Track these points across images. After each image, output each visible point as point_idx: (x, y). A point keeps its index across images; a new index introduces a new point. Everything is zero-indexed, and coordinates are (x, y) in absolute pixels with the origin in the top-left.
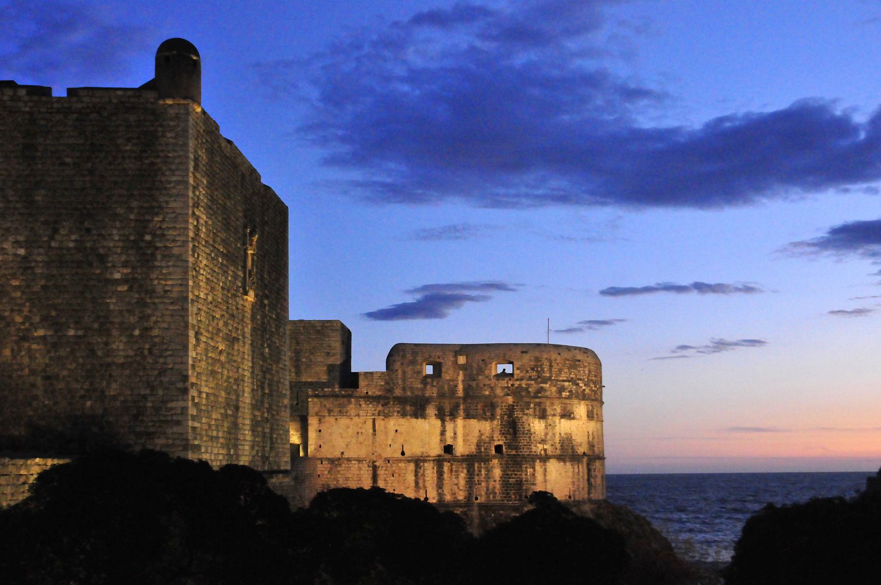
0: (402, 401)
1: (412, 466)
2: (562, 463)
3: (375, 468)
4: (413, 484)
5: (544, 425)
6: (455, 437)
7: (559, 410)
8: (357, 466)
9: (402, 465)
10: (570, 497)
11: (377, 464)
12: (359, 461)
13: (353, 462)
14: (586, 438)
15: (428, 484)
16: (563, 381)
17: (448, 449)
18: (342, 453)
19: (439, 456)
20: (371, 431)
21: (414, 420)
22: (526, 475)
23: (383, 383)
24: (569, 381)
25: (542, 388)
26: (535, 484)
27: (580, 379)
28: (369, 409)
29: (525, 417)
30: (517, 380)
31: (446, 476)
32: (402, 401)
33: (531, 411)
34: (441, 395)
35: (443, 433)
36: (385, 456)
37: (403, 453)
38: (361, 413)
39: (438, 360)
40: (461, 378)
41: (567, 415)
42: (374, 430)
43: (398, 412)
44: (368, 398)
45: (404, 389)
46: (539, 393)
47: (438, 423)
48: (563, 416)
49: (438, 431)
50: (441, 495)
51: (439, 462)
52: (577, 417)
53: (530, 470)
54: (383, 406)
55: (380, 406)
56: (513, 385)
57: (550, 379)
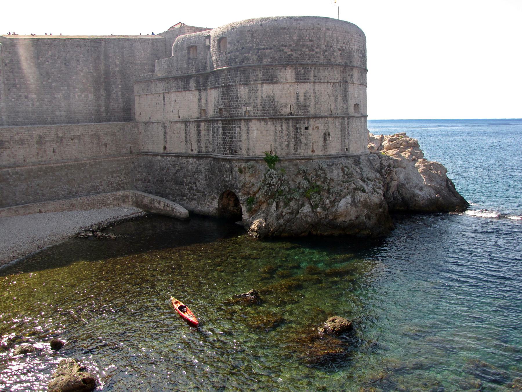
1: (183, 125)
2: (263, 123)
3: (165, 127)
4: (184, 139)
5: (247, 90)
6: (206, 104)
7: (260, 76)
9: (178, 125)
10: (271, 152)
11: (166, 125)
13: (155, 124)
14: (293, 100)
15: (192, 140)
16: (264, 49)
17: (202, 111)
18: (150, 118)
19: (198, 118)
20: (163, 101)
21: (184, 93)
22: (235, 133)
23: (166, 67)
24: (271, 49)
25: (245, 57)
26: (241, 141)
27: (285, 46)
28: (160, 87)
29: (234, 84)
30: (229, 53)
31: (203, 133)
32: (176, 78)
33: (238, 79)
35: (200, 100)
38: (157, 89)
39: (195, 45)
41: (271, 80)
42: (164, 102)
43: (175, 87)
45: (177, 70)
46: (243, 62)
47: (197, 93)
49: (196, 100)
50: (199, 147)
51: (198, 122)
52: (283, 80)
53: (237, 129)
56: (227, 58)
57: (250, 49)
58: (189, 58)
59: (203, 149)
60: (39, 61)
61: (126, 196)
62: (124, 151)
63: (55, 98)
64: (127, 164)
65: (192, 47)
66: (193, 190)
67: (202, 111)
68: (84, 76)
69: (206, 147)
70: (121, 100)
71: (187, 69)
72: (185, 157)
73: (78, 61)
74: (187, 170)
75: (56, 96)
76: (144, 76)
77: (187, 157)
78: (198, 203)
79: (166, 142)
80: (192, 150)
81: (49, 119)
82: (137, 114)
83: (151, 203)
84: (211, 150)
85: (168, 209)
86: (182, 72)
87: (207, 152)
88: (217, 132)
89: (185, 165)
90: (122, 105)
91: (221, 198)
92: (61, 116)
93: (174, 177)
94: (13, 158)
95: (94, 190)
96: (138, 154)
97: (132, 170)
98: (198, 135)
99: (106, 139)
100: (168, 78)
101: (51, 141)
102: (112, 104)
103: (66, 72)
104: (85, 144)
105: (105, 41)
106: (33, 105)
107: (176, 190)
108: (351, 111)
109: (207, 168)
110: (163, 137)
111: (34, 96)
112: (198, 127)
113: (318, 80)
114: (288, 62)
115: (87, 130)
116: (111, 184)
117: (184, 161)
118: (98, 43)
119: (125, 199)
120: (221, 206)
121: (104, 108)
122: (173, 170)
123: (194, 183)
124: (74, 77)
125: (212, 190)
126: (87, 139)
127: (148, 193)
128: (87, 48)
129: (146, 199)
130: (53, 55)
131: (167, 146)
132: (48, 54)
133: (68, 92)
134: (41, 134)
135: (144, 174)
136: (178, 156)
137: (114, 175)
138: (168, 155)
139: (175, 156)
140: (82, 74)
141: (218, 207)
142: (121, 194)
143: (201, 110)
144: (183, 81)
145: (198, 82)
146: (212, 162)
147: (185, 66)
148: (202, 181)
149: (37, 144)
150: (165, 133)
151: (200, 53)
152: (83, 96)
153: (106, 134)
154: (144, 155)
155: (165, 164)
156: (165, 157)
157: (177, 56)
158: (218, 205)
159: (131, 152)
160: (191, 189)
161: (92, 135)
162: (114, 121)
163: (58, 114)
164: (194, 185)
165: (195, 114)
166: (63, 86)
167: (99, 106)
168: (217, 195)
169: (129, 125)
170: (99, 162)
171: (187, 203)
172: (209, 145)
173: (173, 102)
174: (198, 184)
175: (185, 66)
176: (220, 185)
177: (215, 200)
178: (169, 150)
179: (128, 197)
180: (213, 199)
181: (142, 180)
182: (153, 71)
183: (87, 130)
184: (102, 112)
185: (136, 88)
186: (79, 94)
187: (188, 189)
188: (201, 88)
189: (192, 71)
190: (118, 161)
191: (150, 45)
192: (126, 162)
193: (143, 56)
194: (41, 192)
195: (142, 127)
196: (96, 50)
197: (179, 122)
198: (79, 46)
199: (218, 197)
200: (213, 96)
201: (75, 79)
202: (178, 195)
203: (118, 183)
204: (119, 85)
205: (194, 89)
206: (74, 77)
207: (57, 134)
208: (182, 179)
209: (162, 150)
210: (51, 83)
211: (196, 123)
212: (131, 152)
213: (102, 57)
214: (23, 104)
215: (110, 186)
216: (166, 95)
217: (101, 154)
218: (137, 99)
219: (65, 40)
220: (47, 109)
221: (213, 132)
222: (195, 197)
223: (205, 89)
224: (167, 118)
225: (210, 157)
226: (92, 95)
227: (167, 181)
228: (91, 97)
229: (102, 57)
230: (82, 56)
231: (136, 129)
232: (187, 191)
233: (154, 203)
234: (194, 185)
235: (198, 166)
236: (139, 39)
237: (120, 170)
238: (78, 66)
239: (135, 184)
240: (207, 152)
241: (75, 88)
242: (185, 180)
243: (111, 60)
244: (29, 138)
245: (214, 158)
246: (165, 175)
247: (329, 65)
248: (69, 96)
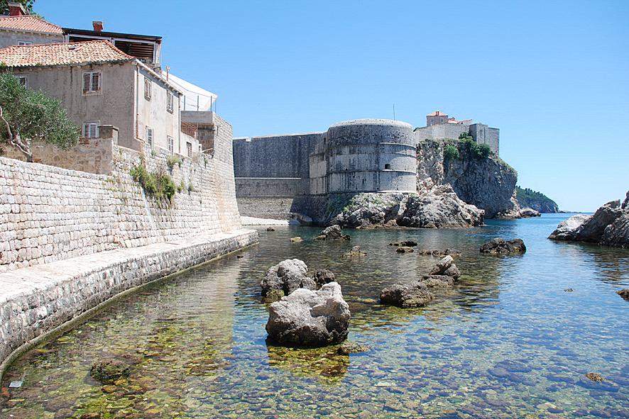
14: (348, 163)
41: (340, 153)
48: (337, 154)
62: (300, 193)
108: (382, 167)
113: (360, 152)
114: (347, 144)
126: (281, 186)
209: (315, 194)
229: (298, 145)
247: (367, 144)
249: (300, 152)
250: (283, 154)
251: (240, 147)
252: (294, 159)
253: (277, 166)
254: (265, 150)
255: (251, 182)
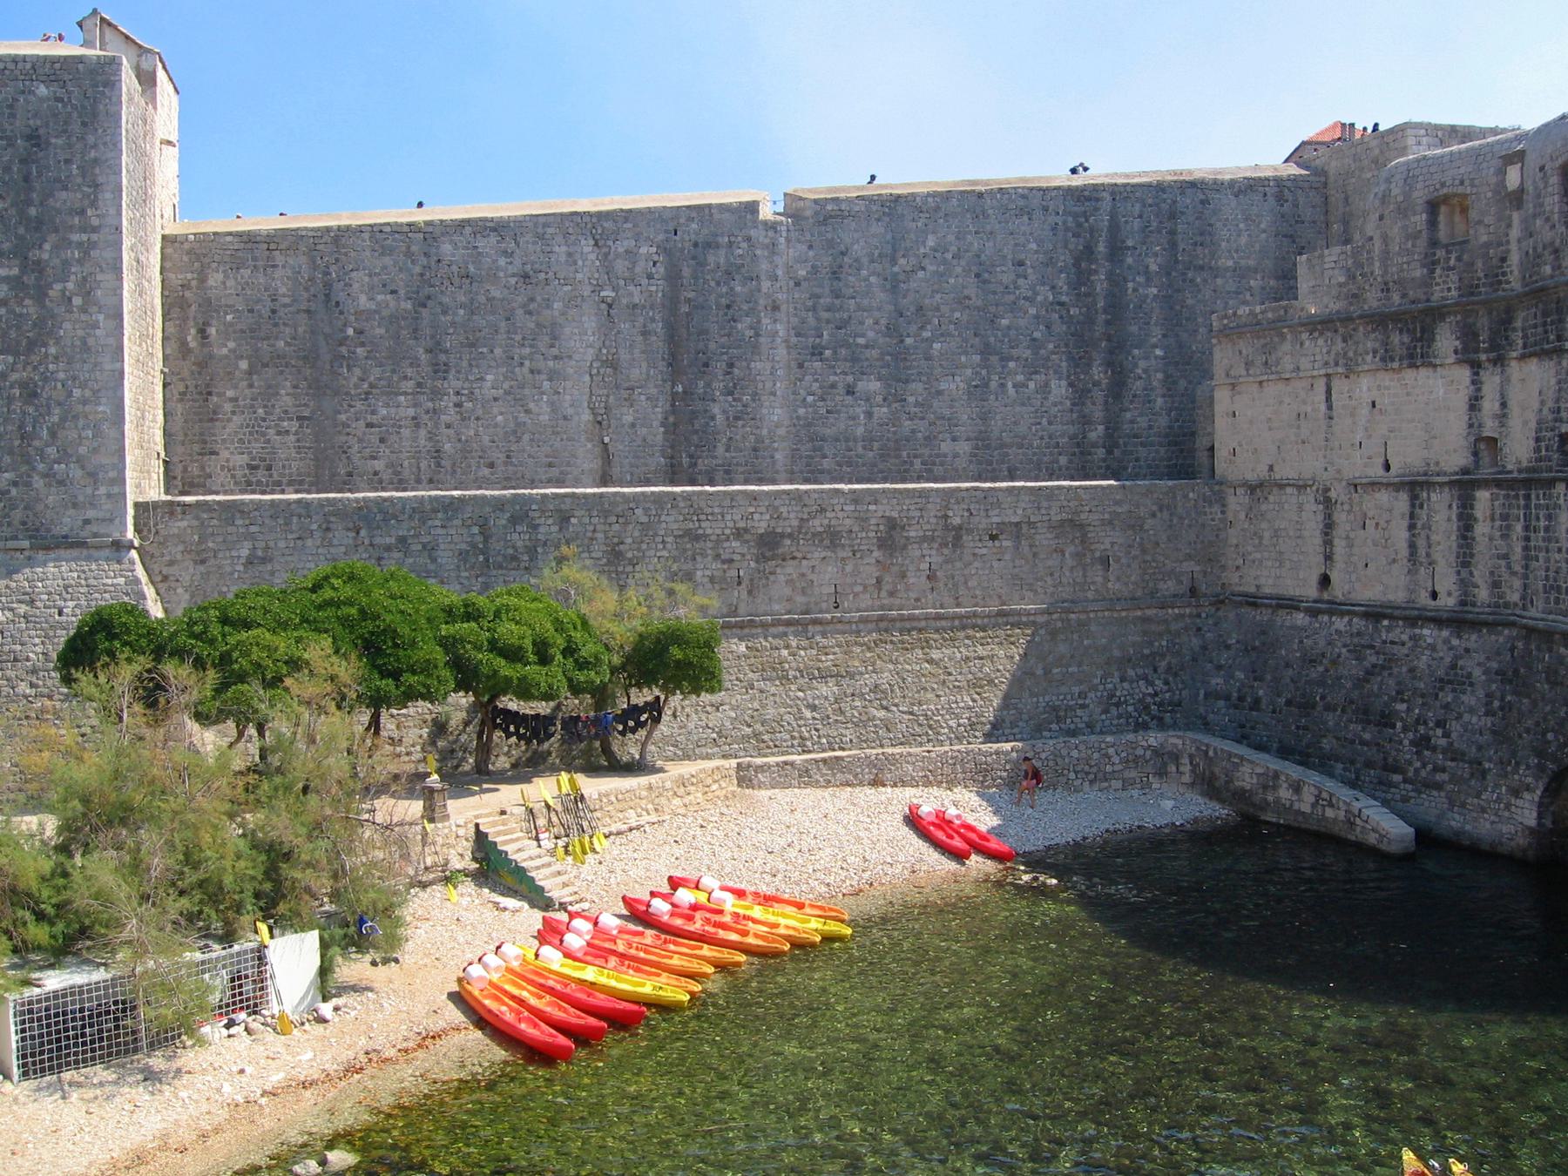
0: (1380, 321)
3: (1328, 503)
8: (1294, 500)
9: (1383, 497)
11: (1333, 494)
12: (1301, 488)
13: (1289, 490)
15: (1437, 556)
17: (1485, 445)
18: (1271, 468)
19: (1465, 471)
20: (1323, 407)
21: (1410, 374)
23: (1342, 279)
28: (1316, 350)
31: (1481, 529)
32: (1380, 321)
34: (1469, 290)
35: (1474, 404)
36: (1349, 473)
37: (1387, 467)
38: (1305, 363)
39: (1460, 190)
40: (1515, 233)
42: (1330, 408)
43: (1375, 352)
44: (1322, 325)
47: (1465, 373)
49: (1460, 400)
50: (1465, 585)
51: (1464, 486)
54: (1345, 341)
55: (1340, 340)
58: (1434, 243)
59: (1483, 594)
60: (896, 269)
61: (1170, 753)
62: (1168, 587)
63: (940, 393)
64: (1178, 634)
65: (1446, 199)
66: (1434, 749)
67: (1482, 446)
68: (1037, 317)
69: (1496, 585)
70: (1160, 401)
71: (1428, 282)
72: (1405, 619)
73: (1021, 264)
74: (1412, 670)
75: (943, 386)
76: (1252, 313)
77: (1415, 618)
78: (1452, 804)
79: (1328, 558)
80: (1434, 595)
81: (917, 463)
82: (1221, 453)
83: (1265, 787)
84: (1515, 597)
85: (1330, 813)
86: (1404, 296)
87: (1499, 604)
88: (1547, 529)
89: (1405, 651)
90: (1163, 421)
91: (1552, 791)
92: (956, 456)
93: (1355, 694)
94: (804, 593)
95: (1059, 720)
96: (1219, 602)
97: (1194, 660)
98: (1465, 538)
99: (1107, 541)
100: (1347, 319)
101: (924, 539)
102: (1128, 415)
103: (979, 303)
104: (1035, 555)
105: (1113, 193)
106: (869, 415)
107: (1363, 743)
109: (1495, 665)
110: (1318, 540)
111: (875, 386)
112: (1464, 506)
115: (1045, 504)
116: (1117, 705)
117: (1401, 633)
118: (1089, 199)
119: (1165, 765)
120: (1548, 822)
121: (1101, 428)
122: (1352, 668)
123: (1440, 724)
124: (1005, 322)
125: (1514, 754)
126: (1044, 538)
127: (1249, 746)
128: (1052, 219)
129: (1246, 769)
130: (941, 248)
131: (1335, 576)
132: (924, 243)
133: (984, 372)
134: (895, 514)
135: (1240, 675)
136: (1375, 614)
137: (1131, 673)
138: (1336, 608)
139: (1366, 615)
140: (1033, 311)
141: (1539, 824)
142: (1152, 742)
143: (1479, 439)
144: (1407, 332)
145: (1468, 336)
146: (1520, 645)
147: (1418, 273)
148: (1471, 718)
149: (879, 547)
150: (1329, 527)
151: (1480, 222)
152: (1032, 385)
153: (1110, 522)
154: (1241, 604)
155: (1322, 643)
156: (1326, 618)
157: (1385, 239)
158: (1540, 816)
159: (1193, 591)
160: (1423, 743)
161: (1063, 521)
162: (1135, 477)
163: (945, 447)
164: (1439, 732)
165: (1453, 456)
166: (966, 353)
167: (1085, 421)
168: (1537, 778)
169: (1193, 491)
170: (1081, 624)
171: (1405, 800)
172: (1506, 576)
173: (1365, 410)
174: (1455, 727)
175: (1418, 273)
176: (1550, 736)
177: (1527, 795)
178: (1338, 590)
179: (1176, 757)
180: (1516, 793)
181: (1227, 698)
182: (1291, 292)
183: (1045, 504)
184: (1094, 445)
185: (1223, 357)
186: (1020, 378)
187: (1412, 743)
188: (1483, 357)
189: (1446, 289)
190: (1146, 620)
191: (1271, 200)
192: (1174, 627)
193: (1243, 240)
194: (882, 714)
195: (1237, 502)
196: (1080, 225)
197: (1388, 485)
198: (1025, 211)
199: (1541, 786)
200: (1536, 387)
201: (1009, 328)
202: (1369, 764)
203: (1140, 701)
204: (1155, 346)
205: (1451, 360)
206: (1005, 322)
207: (946, 517)
208: (1386, 704)
209: (1311, 591)
210: (930, 341)
211: (1455, 493)
212: (1193, 591)
213: (1101, 248)
214: (838, 412)
215: (1114, 711)
216: (1337, 385)
217: (1090, 595)
218: (1222, 397)
219: (980, 195)
220: (913, 431)
221: (1527, 528)
222: (1440, 777)
223: (1499, 361)
224: (1339, 471)
225: (1513, 624)
226: (1064, 383)
227: (1328, 708)
228: (1059, 389)
229: (1101, 248)
230: (1034, 246)
231: (1216, 508)
232: (1406, 752)
233: (1275, 788)
234: (1439, 732)
235: (1456, 658)
236: (1232, 183)
237: (1152, 654)
238: (1021, 281)
239: (1202, 710)
240: (1497, 605)
241: (1005, 359)
242: (1402, 707)
243: (1130, 260)
244: (855, 529)
245: (1530, 631)
246: (1321, 683)
248: (986, 385)
249: (1116, 305)
250: (1013, 307)
251: (716, 258)
252: (1079, 347)
253: (979, 390)
254: (894, 285)
255: (843, 518)
